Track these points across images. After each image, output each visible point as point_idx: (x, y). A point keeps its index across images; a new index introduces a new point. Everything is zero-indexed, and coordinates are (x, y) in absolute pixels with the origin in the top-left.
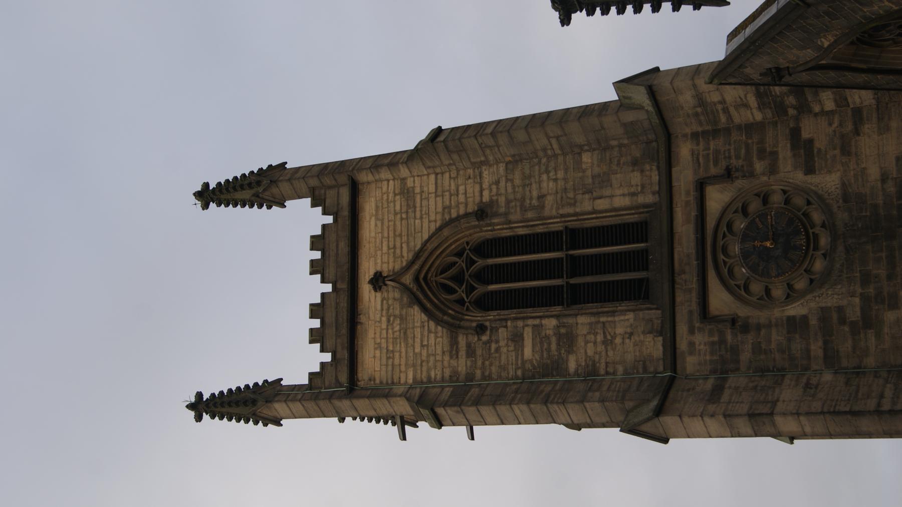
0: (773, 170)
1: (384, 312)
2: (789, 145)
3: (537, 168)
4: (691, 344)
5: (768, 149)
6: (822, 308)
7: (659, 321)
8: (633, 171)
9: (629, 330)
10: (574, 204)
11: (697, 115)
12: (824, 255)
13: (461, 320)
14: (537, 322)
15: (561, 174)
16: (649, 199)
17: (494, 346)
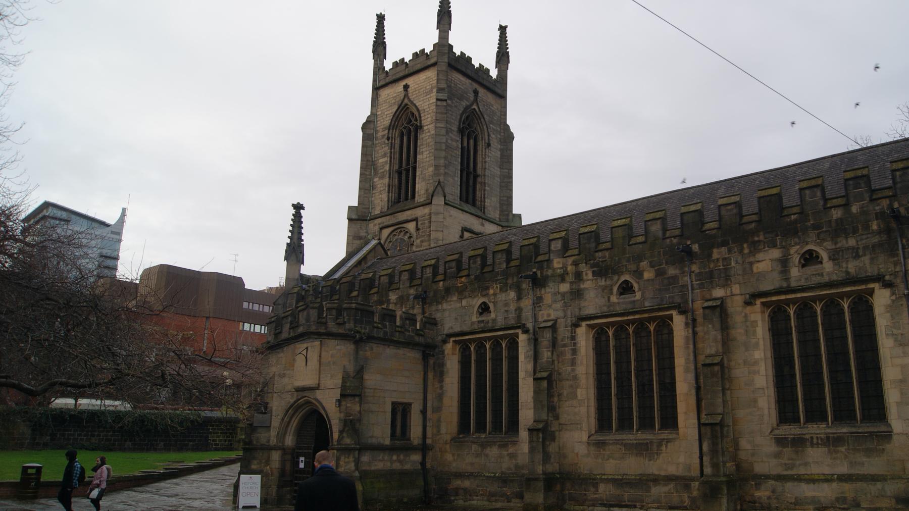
13: (393, 129)
14: (388, 162)
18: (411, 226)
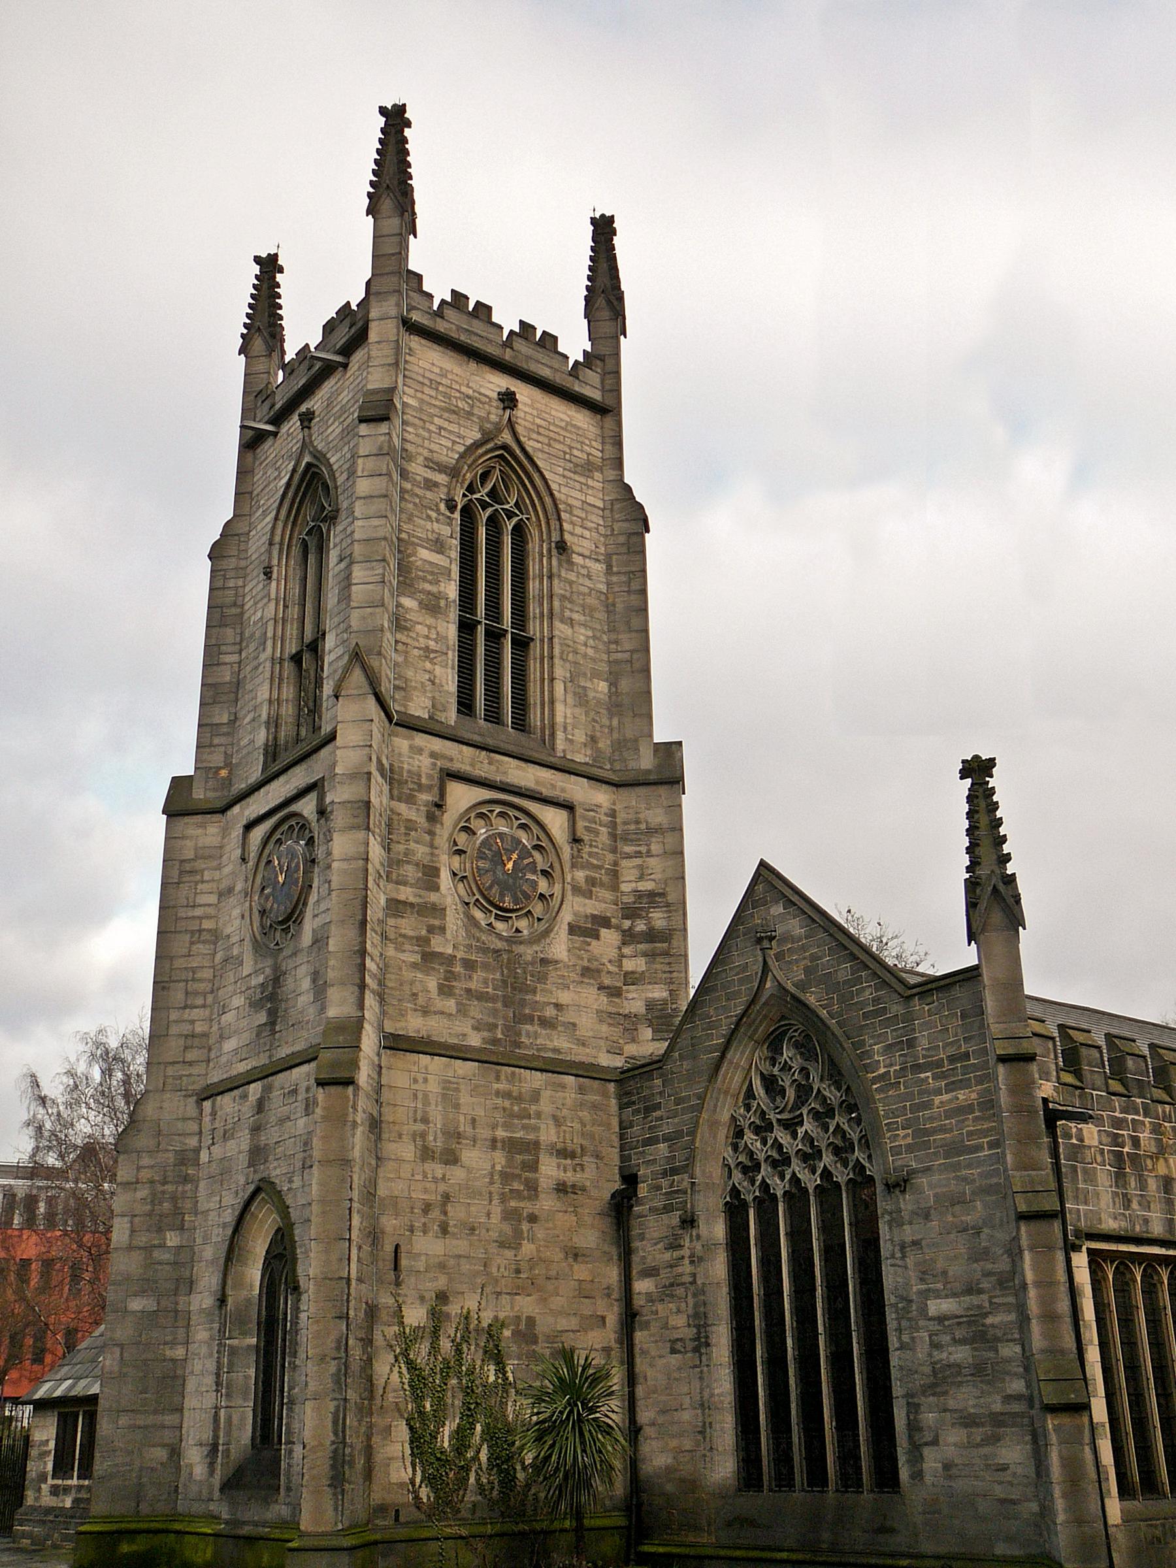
0: (577, 890)
1: (476, 395)
2: (596, 913)
3: (599, 627)
4: (420, 751)
5: (594, 889)
6: (444, 909)
7: (443, 720)
8: (586, 735)
9: (437, 681)
10: (561, 658)
11: (638, 822)
12: (490, 925)
15: (590, 652)
16: (560, 745)
17: (434, 515)
18: (555, 820)
